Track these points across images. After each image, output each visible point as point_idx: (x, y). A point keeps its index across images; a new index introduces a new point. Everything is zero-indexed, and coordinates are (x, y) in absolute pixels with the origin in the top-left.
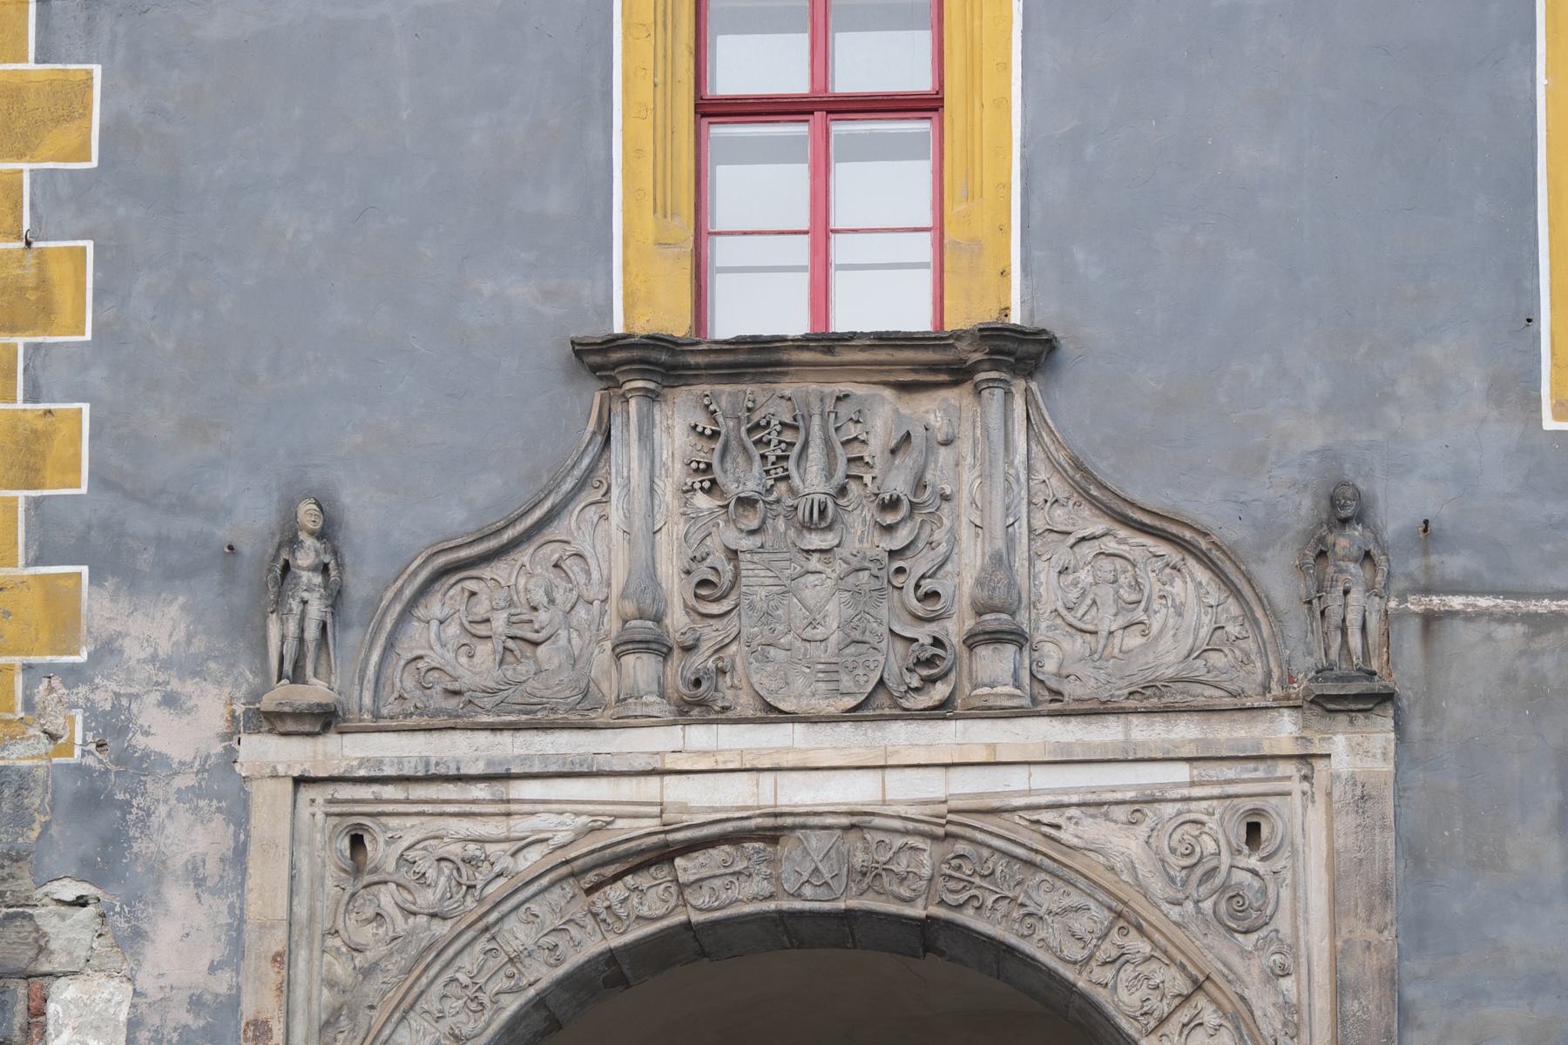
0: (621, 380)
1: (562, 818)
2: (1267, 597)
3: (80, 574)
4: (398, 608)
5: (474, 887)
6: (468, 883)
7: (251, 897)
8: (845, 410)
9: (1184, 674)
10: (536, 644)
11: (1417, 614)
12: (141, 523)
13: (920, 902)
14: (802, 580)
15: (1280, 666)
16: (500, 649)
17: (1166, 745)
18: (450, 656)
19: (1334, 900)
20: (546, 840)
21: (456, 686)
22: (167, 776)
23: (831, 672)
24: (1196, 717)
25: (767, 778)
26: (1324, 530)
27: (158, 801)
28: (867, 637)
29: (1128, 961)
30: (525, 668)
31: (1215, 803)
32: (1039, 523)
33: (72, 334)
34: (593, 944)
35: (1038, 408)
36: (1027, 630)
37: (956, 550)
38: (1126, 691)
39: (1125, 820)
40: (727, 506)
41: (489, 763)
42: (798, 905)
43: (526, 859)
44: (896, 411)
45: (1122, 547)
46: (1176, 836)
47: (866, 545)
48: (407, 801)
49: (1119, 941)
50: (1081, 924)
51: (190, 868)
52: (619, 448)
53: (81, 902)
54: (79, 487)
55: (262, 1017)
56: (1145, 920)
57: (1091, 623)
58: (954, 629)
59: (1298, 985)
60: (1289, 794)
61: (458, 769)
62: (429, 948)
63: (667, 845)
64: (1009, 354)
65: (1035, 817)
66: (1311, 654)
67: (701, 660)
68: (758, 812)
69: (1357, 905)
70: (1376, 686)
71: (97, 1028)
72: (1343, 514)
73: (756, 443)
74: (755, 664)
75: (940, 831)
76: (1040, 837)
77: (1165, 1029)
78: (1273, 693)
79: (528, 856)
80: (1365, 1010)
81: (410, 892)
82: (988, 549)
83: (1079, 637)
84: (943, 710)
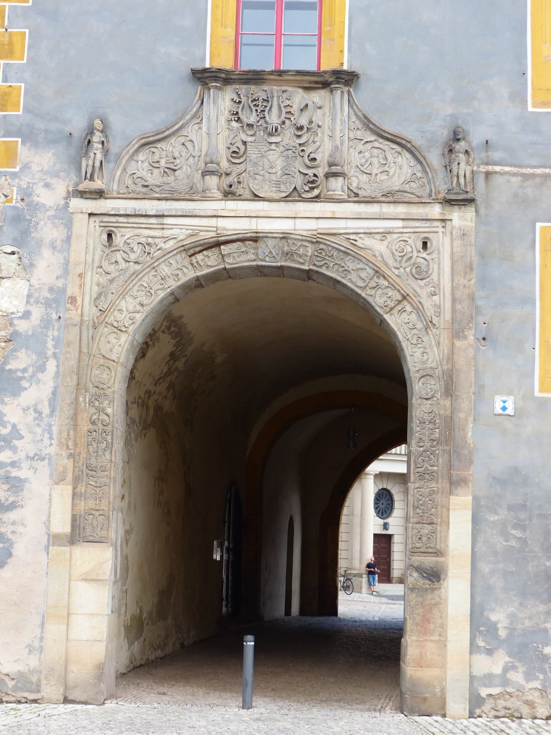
0: (208, 82)
1: (181, 231)
2: (431, 164)
3: (18, 141)
4: (127, 157)
5: (150, 253)
6: (148, 252)
7: (72, 254)
8: (285, 95)
9: (402, 189)
10: (175, 170)
11: (483, 172)
12: (40, 124)
13: (307, 264)
14: (268, 152)
15: (435, 188)
16: (162, 172)
17: (395, 214)
18: (145, 173)
19: (452, 269)
20: (176, 238)
21: (146, 184)
22: (44, 211)
23: (278, 183)
24: (405, 205)
25: (254, 220)
26: (451, 142)
27: (41, 219)
28: (290, 173)
29: (380, 288)
30: (171, 178)
31: (411, 234)
32: (352, 136)
33: (19, 60)
34: (190, 275)
35: (352, 97)
36: (347, 172)
37: (322, 144)
38: (381, 194)
39: (380, 239)
40: (243, 126)
41: (157, 211)
42: (264, 263)
43: (168, 244)
44: (303, 96)
45: (381, 145)
46: (398, 245)
47: (291, 141)
48: (128, 223)
49: (377, 280)
50: (363, 274)
51: (51, 243)
52: (206, 105)
53: (13, 253)
54: (19, 111)
55: (74, 296)
56: (386, 274)
57: (369, 170)
58: (321, 172)
59: (440, 298)
60: (437, 232)
61: (146, 212)
62: (133, 274)
63: (218, 241)
64: (343, 79)
65: (348, 237)
66: (446, 184)
67: (232, 179)
68: (251, 231)
69: (461, 272)
70: (469, 196)
71: (16, 297)
72: (458, 137)
73: (254, 105)
74: (251, 181)
75: (315, 240)
76: (350, 244)
77: (393, 312)
78: (433, 197)
79: (169, 243)
80: (463, 308)
81: (127, 254)
82: (333, 144)
83: (365, 175)
84: (317, 199)
